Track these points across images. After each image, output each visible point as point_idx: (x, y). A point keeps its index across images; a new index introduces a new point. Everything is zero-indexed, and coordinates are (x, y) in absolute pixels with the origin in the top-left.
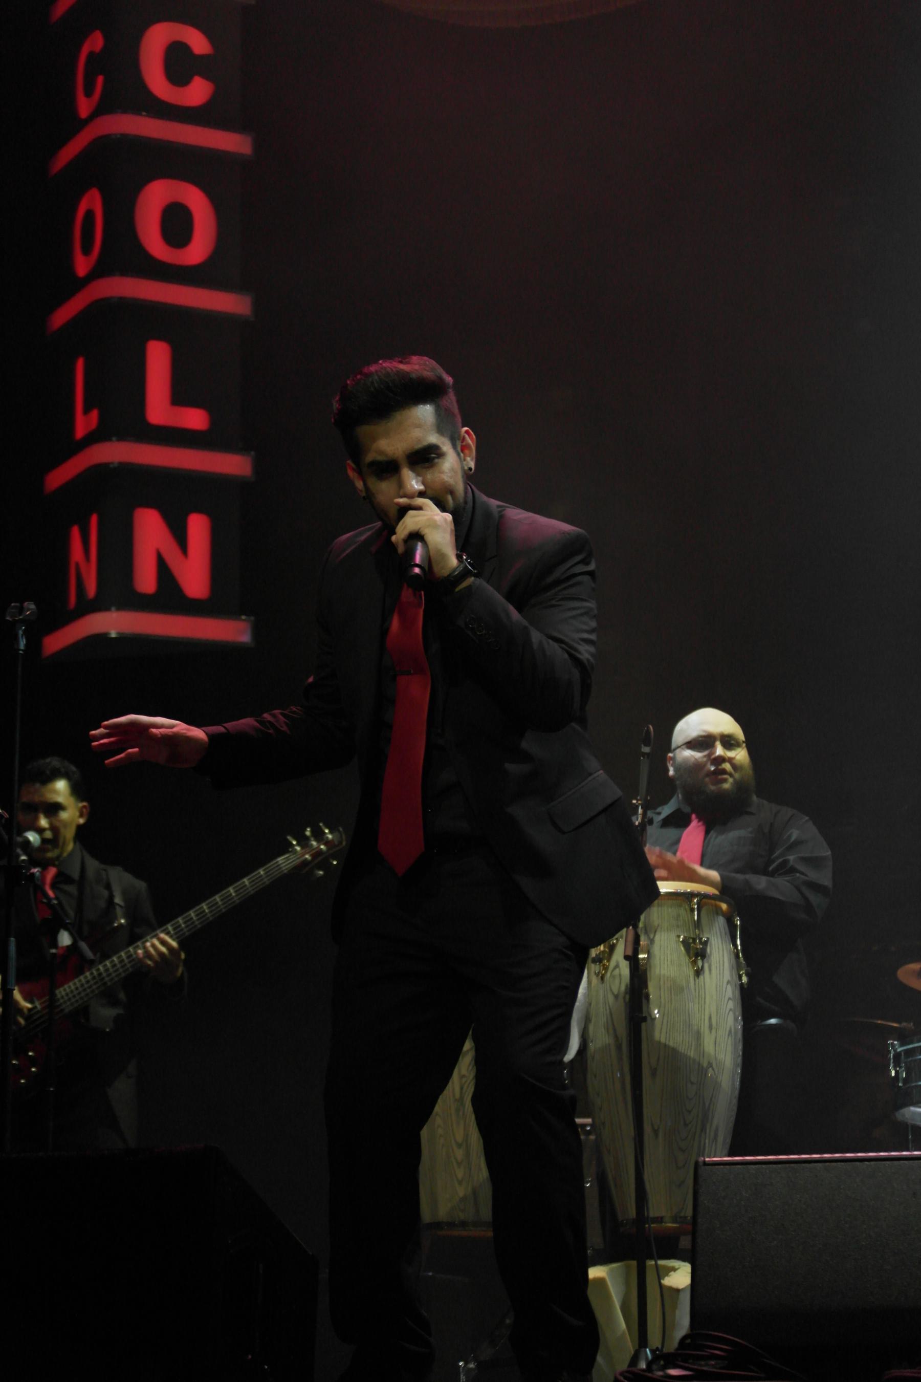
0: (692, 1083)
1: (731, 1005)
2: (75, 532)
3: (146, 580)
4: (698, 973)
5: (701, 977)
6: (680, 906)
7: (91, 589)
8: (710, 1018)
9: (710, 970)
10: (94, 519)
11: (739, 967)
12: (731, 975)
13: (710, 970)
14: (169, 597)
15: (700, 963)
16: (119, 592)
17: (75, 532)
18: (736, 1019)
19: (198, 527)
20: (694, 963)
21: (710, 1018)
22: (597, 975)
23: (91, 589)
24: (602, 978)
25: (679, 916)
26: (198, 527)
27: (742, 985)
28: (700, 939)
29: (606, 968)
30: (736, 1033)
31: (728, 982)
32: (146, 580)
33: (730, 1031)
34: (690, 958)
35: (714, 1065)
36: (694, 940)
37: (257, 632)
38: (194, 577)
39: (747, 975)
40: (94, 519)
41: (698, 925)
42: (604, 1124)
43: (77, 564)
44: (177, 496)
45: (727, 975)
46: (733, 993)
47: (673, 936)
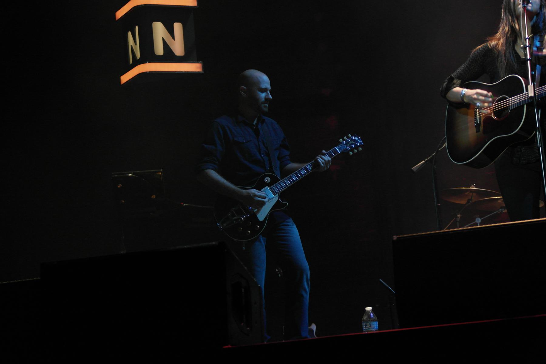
2: (130, 33)
3: (159, 50)
7: (138, 56)
10: (137, 27)
14: (169, 56)
16: (149, 55)
17: (130, 33)
19: (178, 27)
23: (138, 56)
26: (178, 27)
32: (159, 50)
37: (204, 67)
38: (178, 47)
40: (137, 27)
43: (131, 46)
44: (169, 15)
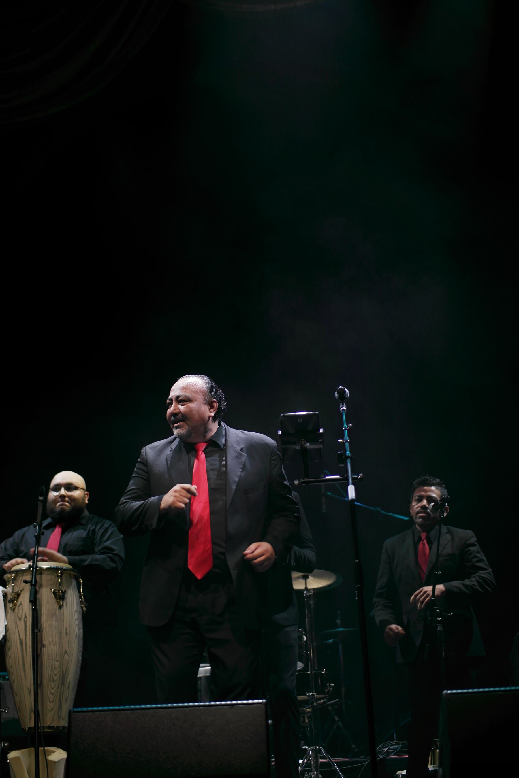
0: (57, 661)
1: (77, 622)
4: (60, 607)
5: (62, 609)
6: (52, 574)
8: (66, 629)
9: (67, 605)
11: (81, 602)
12: (77, 608)
13: (67, 605)
15: (61, 602)
18: (79, 629)
20: (59, 602)
21: (66, 629)
22: (11, 608)
24: (14, 610)
25: (51, 579)
27: (83, 612)
28: (62, 591)
29: (15, 605)
30: (79, 636)
31: (76, 611)
33: (76, 635)
34: (57, 599)
35: (68, 652)
36: (59, 591)
39: (86, 607)
41: (60, 584)
42: (14, 681)
45: (75, 608)
46: (78, 616)
47: (49, 589)
